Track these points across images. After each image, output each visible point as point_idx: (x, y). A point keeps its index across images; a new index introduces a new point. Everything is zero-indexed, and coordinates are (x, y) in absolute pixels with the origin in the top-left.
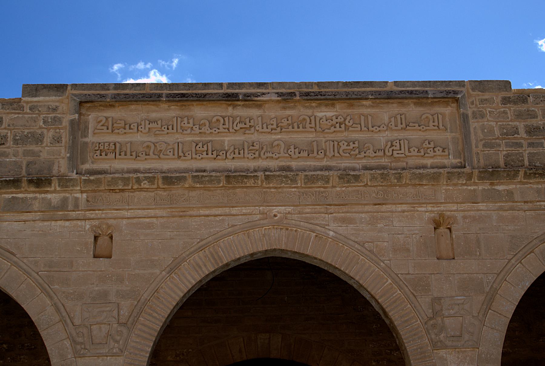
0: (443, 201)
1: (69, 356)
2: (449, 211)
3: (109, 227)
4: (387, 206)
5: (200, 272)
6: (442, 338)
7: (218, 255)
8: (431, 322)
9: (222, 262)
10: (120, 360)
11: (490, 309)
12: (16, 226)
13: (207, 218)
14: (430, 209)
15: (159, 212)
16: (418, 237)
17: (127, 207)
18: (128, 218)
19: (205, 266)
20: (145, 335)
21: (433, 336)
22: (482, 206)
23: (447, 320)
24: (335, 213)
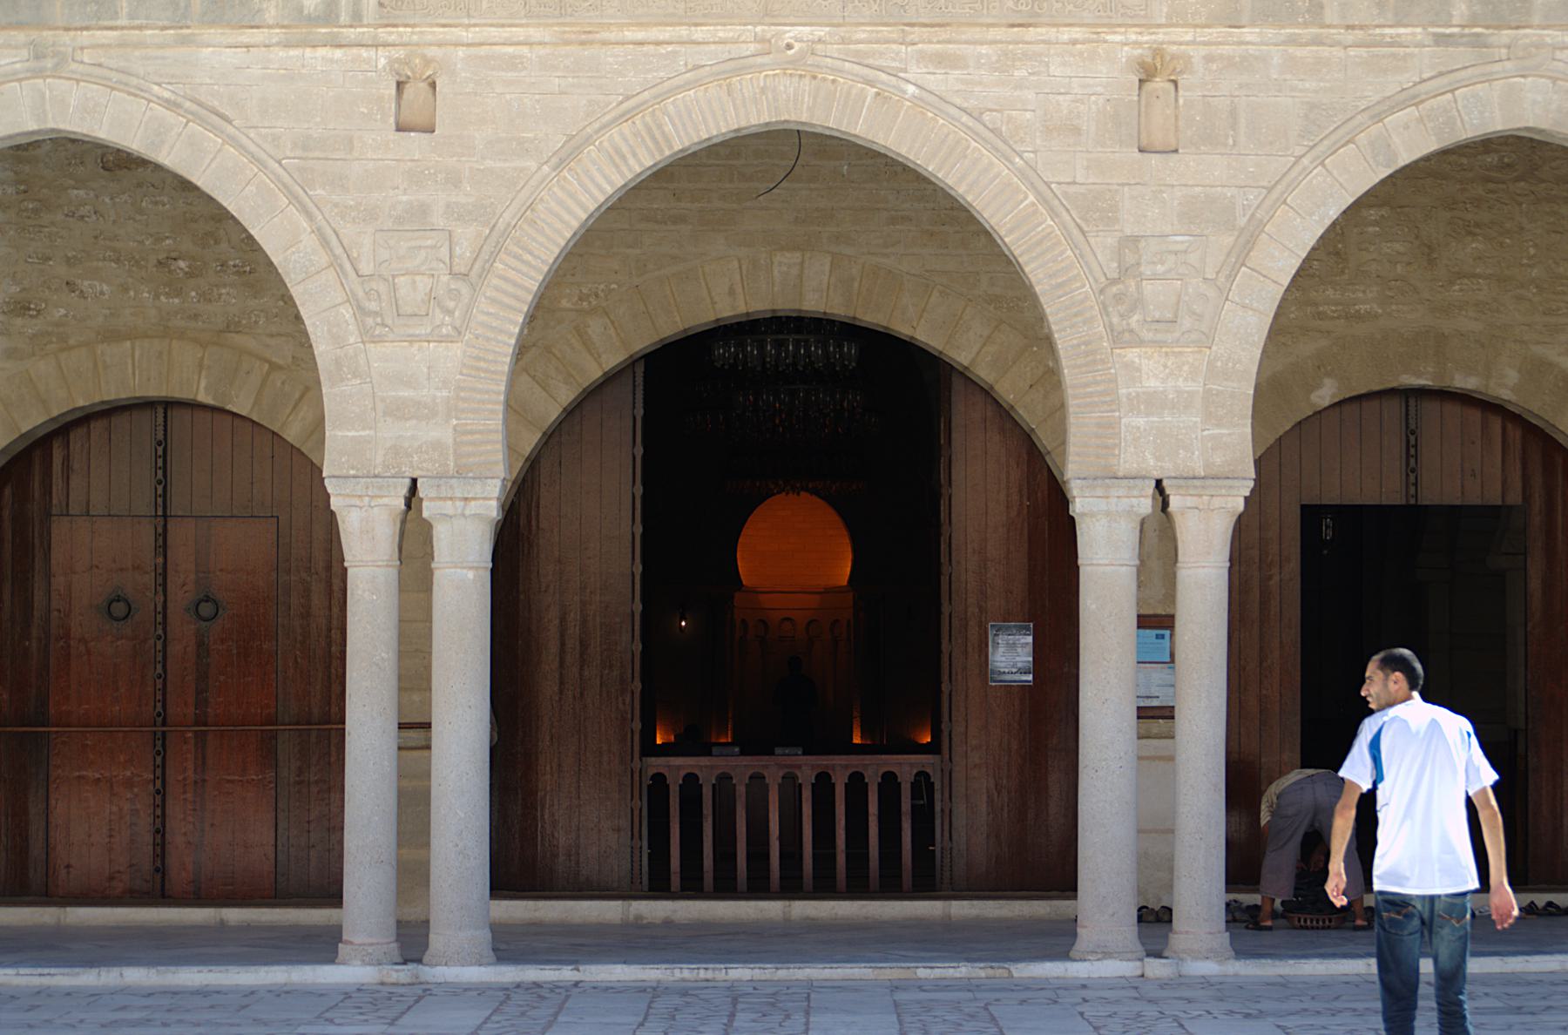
0: (1163, 21)
1: (352, 340)
2: (1174, 43)
3: (427, 62)
4: (1039, 30)
5: (624, 169)
6: (1134, 325)
7: (663, 133)
8: (1114, 289)
9: (671, 147)
10: (457, 350)
11: (1243, 264)
12: (231, 57)
13: (639, 48)
14: (1133, 37)
15: (535, 33)
16: (1101, 100)
17: (466, 21)
18: (468, 45)
19: (635, 155)
20: (506, 300)
21: (1115, 320)
22: (1249, 34)
24: (923, 42)
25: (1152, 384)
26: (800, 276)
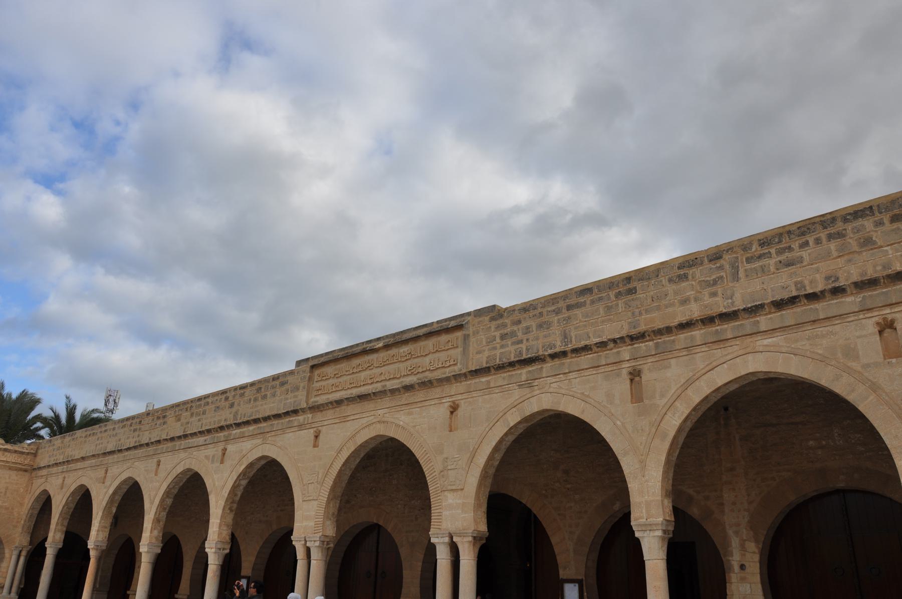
23: (450, 472)
25: (450, 501)
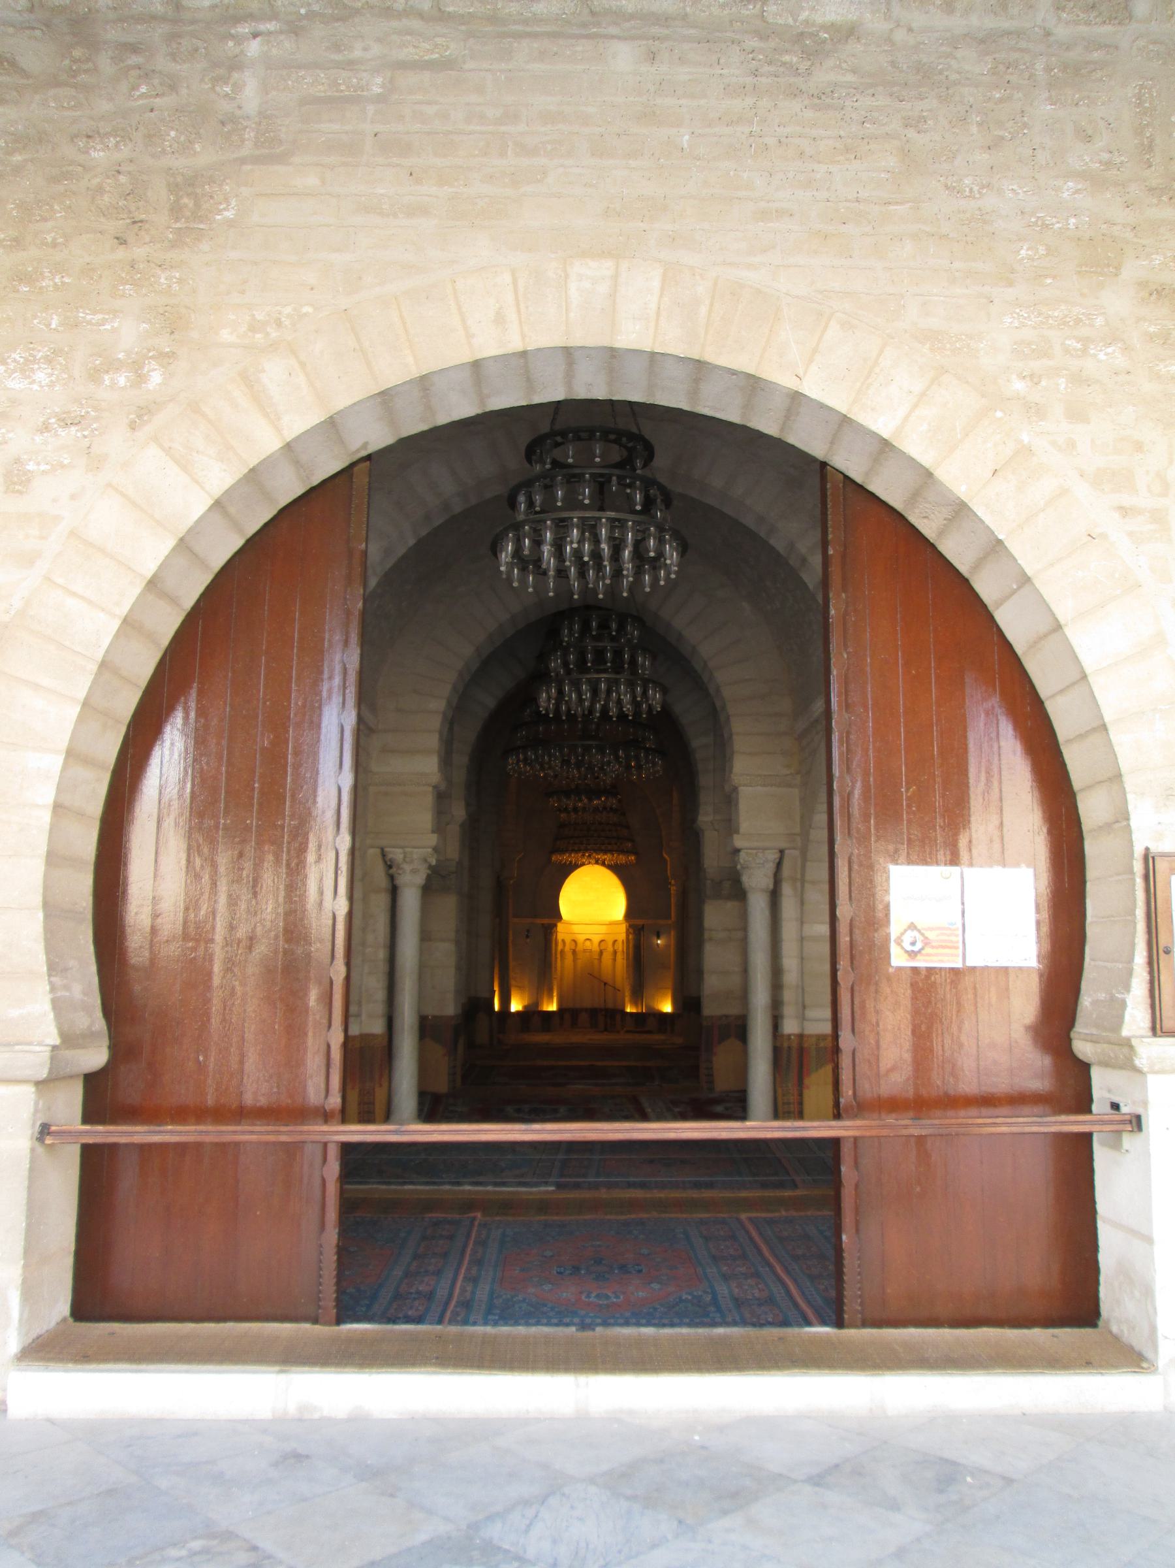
26: (613, 295)
